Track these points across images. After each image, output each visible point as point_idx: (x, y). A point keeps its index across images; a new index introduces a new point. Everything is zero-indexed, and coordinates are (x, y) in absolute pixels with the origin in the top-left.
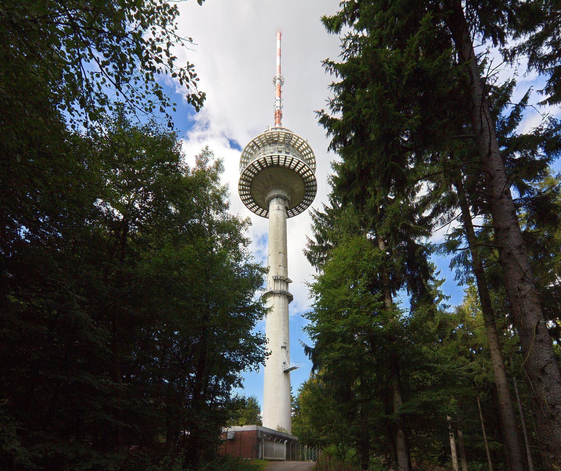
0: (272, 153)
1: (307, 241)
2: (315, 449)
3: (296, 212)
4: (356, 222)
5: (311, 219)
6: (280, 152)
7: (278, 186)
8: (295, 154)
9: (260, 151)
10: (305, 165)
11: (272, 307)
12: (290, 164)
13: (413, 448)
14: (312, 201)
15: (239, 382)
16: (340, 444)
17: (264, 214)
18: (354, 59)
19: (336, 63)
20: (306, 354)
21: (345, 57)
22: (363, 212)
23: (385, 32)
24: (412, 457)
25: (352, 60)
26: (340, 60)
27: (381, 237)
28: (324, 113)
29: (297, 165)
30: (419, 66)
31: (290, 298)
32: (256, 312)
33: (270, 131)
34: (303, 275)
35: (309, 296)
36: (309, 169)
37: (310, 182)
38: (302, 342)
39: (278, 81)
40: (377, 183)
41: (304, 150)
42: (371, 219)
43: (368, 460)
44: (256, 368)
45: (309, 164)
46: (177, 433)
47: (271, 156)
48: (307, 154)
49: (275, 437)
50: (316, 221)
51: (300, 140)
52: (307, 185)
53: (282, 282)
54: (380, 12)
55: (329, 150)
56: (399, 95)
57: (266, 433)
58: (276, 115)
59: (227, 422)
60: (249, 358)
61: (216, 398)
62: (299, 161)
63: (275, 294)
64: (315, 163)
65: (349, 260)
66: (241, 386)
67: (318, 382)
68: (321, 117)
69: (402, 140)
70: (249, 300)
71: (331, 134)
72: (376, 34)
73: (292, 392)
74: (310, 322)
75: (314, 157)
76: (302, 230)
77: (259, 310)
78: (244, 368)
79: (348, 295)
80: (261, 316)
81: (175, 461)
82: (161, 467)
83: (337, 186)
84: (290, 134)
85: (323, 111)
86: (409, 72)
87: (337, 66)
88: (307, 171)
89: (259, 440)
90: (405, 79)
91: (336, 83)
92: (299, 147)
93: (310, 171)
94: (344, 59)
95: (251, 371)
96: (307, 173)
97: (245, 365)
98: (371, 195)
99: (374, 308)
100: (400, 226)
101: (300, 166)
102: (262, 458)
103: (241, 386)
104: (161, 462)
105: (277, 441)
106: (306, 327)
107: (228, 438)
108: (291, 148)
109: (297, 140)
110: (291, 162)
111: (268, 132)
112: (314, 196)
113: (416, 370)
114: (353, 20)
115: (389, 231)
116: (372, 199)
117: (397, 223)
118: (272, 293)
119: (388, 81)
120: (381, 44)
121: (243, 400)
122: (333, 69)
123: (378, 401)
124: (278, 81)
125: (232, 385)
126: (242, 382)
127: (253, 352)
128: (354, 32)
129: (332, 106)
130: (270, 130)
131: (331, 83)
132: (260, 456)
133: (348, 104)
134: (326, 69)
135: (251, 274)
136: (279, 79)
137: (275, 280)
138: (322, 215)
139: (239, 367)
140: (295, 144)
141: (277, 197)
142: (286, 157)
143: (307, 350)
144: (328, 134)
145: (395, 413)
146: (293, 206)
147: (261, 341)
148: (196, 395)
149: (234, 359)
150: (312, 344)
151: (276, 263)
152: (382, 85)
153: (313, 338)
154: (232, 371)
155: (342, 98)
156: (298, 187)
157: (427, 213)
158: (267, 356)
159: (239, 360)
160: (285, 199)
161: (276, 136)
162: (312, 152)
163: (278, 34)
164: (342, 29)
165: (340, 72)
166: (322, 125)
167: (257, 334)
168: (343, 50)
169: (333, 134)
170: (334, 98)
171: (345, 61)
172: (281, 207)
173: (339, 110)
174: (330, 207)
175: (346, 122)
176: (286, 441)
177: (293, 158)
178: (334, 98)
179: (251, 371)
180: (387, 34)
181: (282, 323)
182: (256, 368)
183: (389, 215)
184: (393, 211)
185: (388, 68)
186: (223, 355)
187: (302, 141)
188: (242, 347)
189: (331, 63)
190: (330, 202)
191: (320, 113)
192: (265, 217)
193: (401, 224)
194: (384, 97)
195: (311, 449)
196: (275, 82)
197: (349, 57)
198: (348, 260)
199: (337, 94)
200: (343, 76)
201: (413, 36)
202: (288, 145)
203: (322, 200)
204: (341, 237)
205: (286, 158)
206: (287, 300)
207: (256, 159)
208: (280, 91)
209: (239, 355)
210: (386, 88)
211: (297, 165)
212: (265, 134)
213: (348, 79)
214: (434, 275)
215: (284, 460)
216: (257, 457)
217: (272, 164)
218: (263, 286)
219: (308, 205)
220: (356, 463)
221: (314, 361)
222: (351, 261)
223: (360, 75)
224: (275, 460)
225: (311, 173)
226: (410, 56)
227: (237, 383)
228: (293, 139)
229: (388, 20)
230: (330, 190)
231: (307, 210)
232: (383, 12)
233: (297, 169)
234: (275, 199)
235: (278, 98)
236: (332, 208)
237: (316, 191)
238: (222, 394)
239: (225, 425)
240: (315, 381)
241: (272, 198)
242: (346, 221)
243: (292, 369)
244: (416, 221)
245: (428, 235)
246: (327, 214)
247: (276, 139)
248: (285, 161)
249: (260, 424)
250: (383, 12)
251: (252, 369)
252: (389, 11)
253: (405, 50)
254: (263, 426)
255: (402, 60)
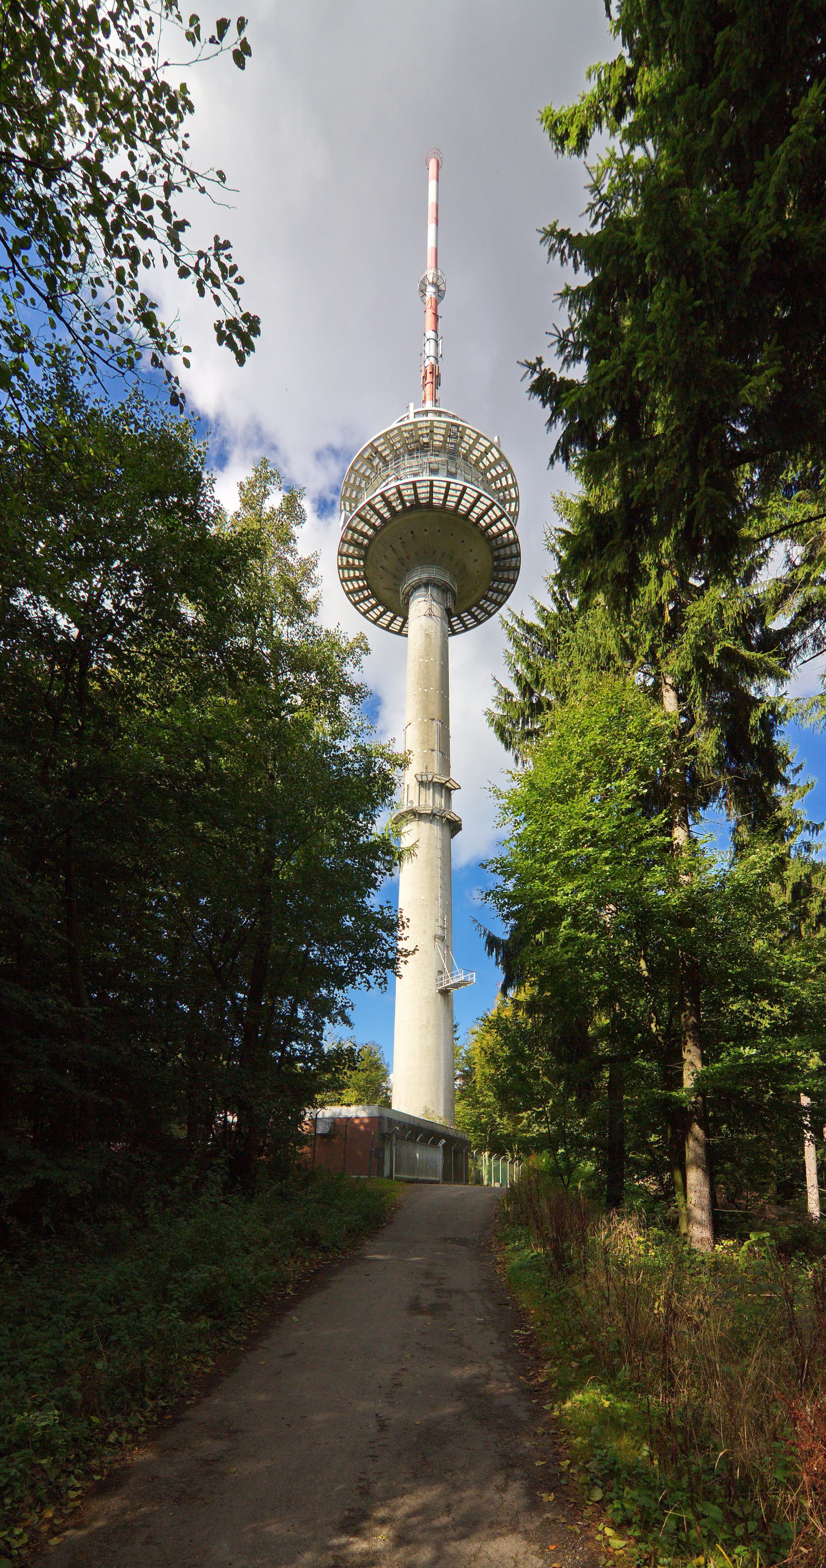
0: (415, 475)
1: (495, 692)
2: (505, 1160)
3: (470, 621)
4: (612, 646)
5: (505, 638)
6: (434, 472)
7: (428, 557)
8: (469, 477)
9: (389, 472)
10: (493, 504)
11: (415, 845)
12: (458, 503)
13: (722, 1165)
14: (507, 594)
15: (341, 1013)
16: (561, 1151)
17: (396, 626)
18: (621, 220)
19: (574, 233)
20: (490, 953)
21: (598, 215)
22: (628, 621)
23: (701, 146)
24: (719, 1183)
25: (614, 224)
26: (585, 226)
27: (669, 680)
28: (543, 367)
29: (474, 505)
30: (784, 234)
31: (454, 827)
32: (378, 859)
33: (412, 419)
34: (487, 772)
35: (498, 820)
36: (503, 515)
37: (504, 546)
38: (480, 925)
39: (431, 290)
40: (666, 545)
41: (492, 466)
42: (649, 637)
43: (622, 1187)
44: (380, 981)
45: (503, 502)
46: (210, 1118)
47: (414, 483)
48: (498, 477)
49: (418, 1132)
50: (516, 642)
51: (481, 440)
52: (496, 554)
53: (438, 788)
54: (689, 89)
55: (552, 462)
56: (730, 313)
57: (399, 1123)
58: (425, 377)
59: (318, 1097)
60: (364, 959)
61: (291, 1046)
62: (480, 495)
63: (420, 815)
64: (517, 499)
65: (594, 737)
66: (347, 1021)
67: (515, 1015)
68: (536, 376)
69: (733, 432)
70: (365, 830)
71: (559, 421)
72: (679, 149)
73: (456, 1036)
74: (500, 880)
75: (515, 485)
76: (483, 665)
77: (387, 853)
78: (353, 980)
79: (589, 818)
80: (390, 866)
81: (206, 1177)
82: (178, 1189)
83: (570, 556)
84: (458, 426)
85: (540, 361)
86: (760, 251)
87: (576, 242)
88: (499, 519)
89: (384, 1137)
90: (750, 269)
91: (574, 288)
92: (479, 460)
93: (504, 520)
94: (595, 222)
95: (370, 987)
96: (499, 524)
97: (355, 974)
98: (649, 578)
99: (648, 850)
100: (716, 653)
101: (481, 506)
102: (391, 1177)
103: (347, 1021)
104: (177, 1179)
105: (424, 1141)
106: (491, 892)
107: (319, 1132)
108: (460, 461)
109: (476, 441)
110: (461, 498)
111: (406, 421)
112: (514, 582)
113: (736, 992)
114: (619, 114)
115: (689, 665)
116: (652, 585)
117: (709, 646)
118: (416, 814)
119: (704, 277)
120: (690, 180)
121: (351, 1051)
122: (566, 251)
123: (648, 1060)
124: (431, 290)
125: (326, 1020)
126: (348, 1011)
127: (373, 947)
128: (620, 148)
129: (562, 348)
130: (412, 415)
131: (562, 289)
132: (387, 1172)
133: (602, 343)
134: (551, 250)
135: (368, 768)
136: (434, 284)
137: (421, 783)
138: (530, 629)
139: (342, 979)
140: (470, 451)
141: (427, 584)
142: (449, 483)
143: (492, 943)
144: (551, 422)
145: (685, 1086)
146: (466, 605)
147: (392, 925)
148: (248, 1037)
149: (331, 962)
150: (503, 931)
151: (425, 742)
152: (689, 285)
153: (507, 917)
154: (327, 987)
155: (588, 325)
156: (478, 560)
157: (779, 622)
158: (406, 956)
159: (342, 964)
160: (444, 589)
161: (425, 431)
162: (510, 470)
163: (432, 164)
164: (591, 142)
165: (585, 257)
166: (537, 399)
167: (381, 907)
168: (591, 199)
169: (564, 420)
170: (568, 326)
171: (598, 228)
172: (437, 610)
173: (580, 357)
174: (552, 607)
175: (597, 389)
176: (444, 1141)
177: (465, 488)
178: (567, 326)
179: (370, 987)
180: (707, 150)
181: (439, 882)
182: (380, 981)
183: (691, 626)
184: (700, 618)
185: (705, 240)
186: (307, 952)
187: (487, 444)
188: (347, 934)
189: (564, 235)
190: (549, 596)
191: (532, 367)
192: (399, 633)
193: (717, 648)
194: (692, 319)
195: (497, 1159)
196: (423, 291)
197: (607, 216)
198: (590, 735)
199: (574, 317)
200: (590, 268)
201: (772, 152)
202: (453, 454)
203: (533, 593)
204: (575, 682)
205: (448, 488)
206: (447, 830)
207: (379, 491)
208: (436, 317)
209: (341, 952)
210: (697, 295)
211: (474, 505)
212: (399, 428)
213: (604, 275)
214: (787, 772)
215: (437, 1182)
216: (380, 1173)
217: (416, 505)
218: (394, 798)
219: (500, 605)
220: (594, 1192)
221: (508, 969)
222: (599, 739)
223: (634, 263)
224: (424, 1182)
225: (507, 525)
226: (761, 207)
227: (337, 1014)
228: (466, 438)
229: (710, 110)
230: (554, 568)
231: (497, 614)
232: (700, 87)
233: (474, 516)
234: (422, 591)
235: (430, 334)
236: (556, 610)
237: (517, 569)
238: (306, 1038)
239: (313, 1104)
240: (508, 1013)
241: (416, 588)
242: (589, 642)
243: (456, 986)
244: (753, 642)
245: (781, 678)
246: (543, 626)
247: (426, 440)
248: (446, 494)
249: (387, 1103)
250: (700, 87)
251: (372, 984)
252: (714, 85)
253: (750, 192)
254: (394, 1107)
255: (742, 220)
